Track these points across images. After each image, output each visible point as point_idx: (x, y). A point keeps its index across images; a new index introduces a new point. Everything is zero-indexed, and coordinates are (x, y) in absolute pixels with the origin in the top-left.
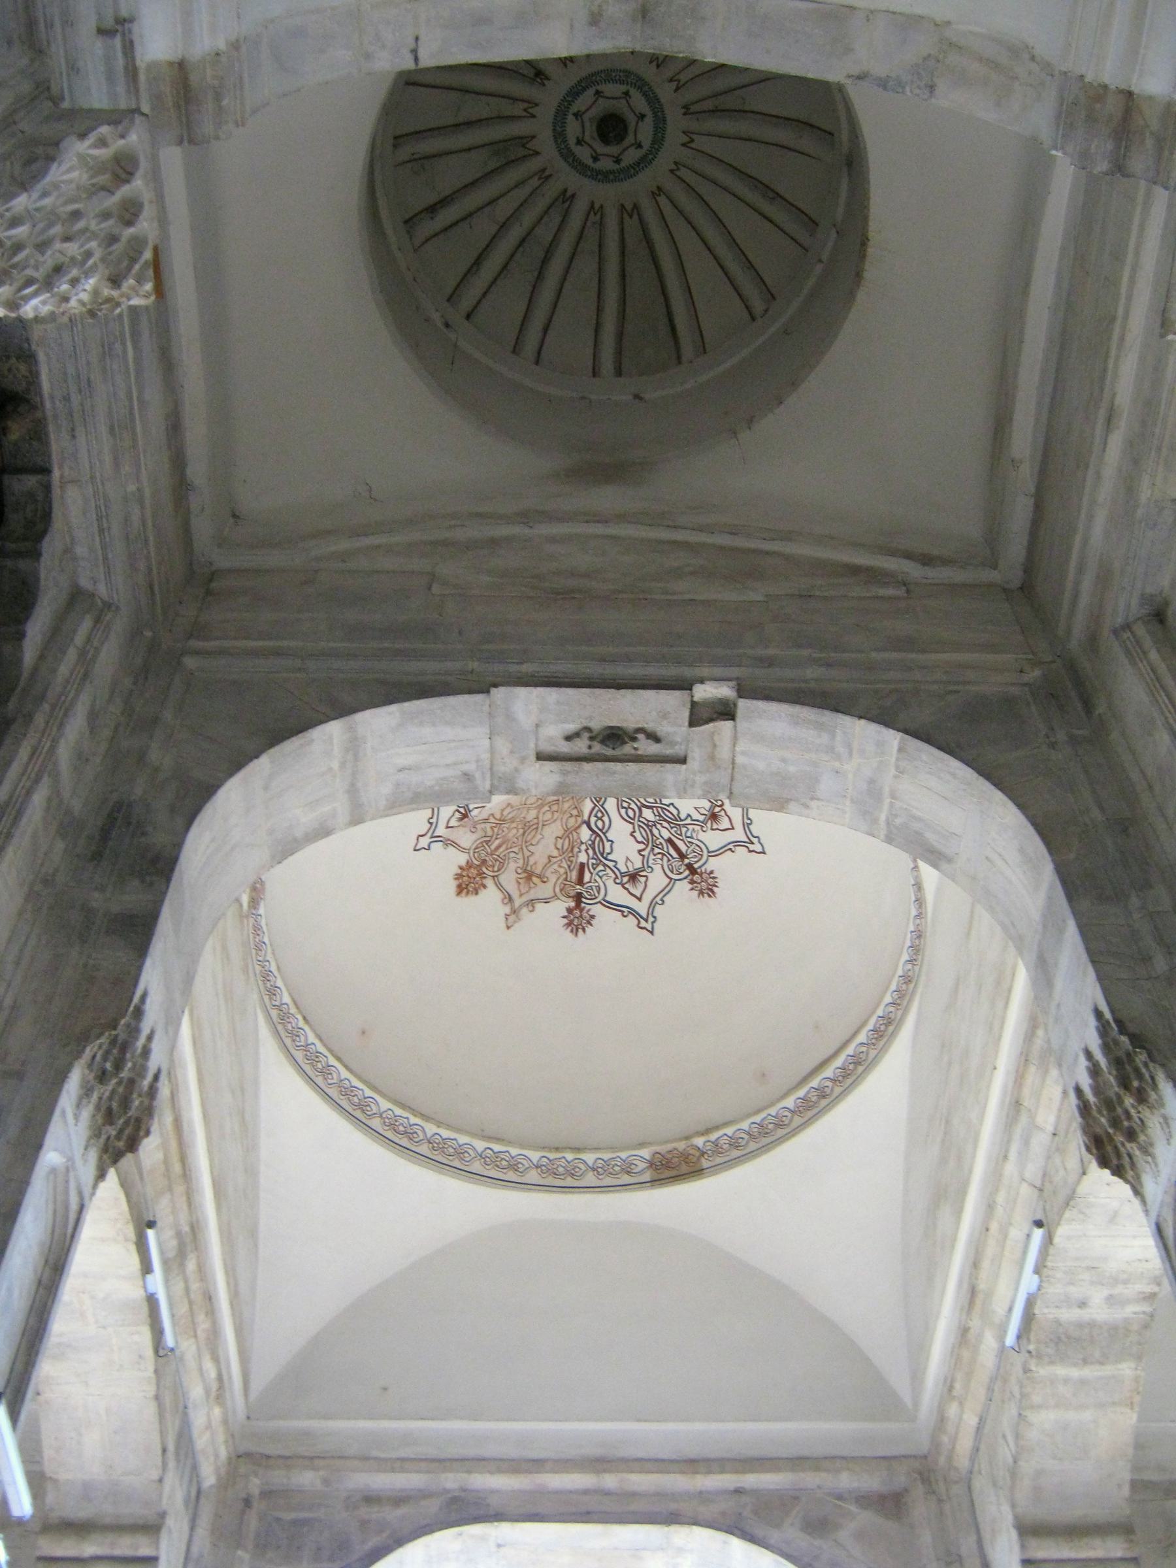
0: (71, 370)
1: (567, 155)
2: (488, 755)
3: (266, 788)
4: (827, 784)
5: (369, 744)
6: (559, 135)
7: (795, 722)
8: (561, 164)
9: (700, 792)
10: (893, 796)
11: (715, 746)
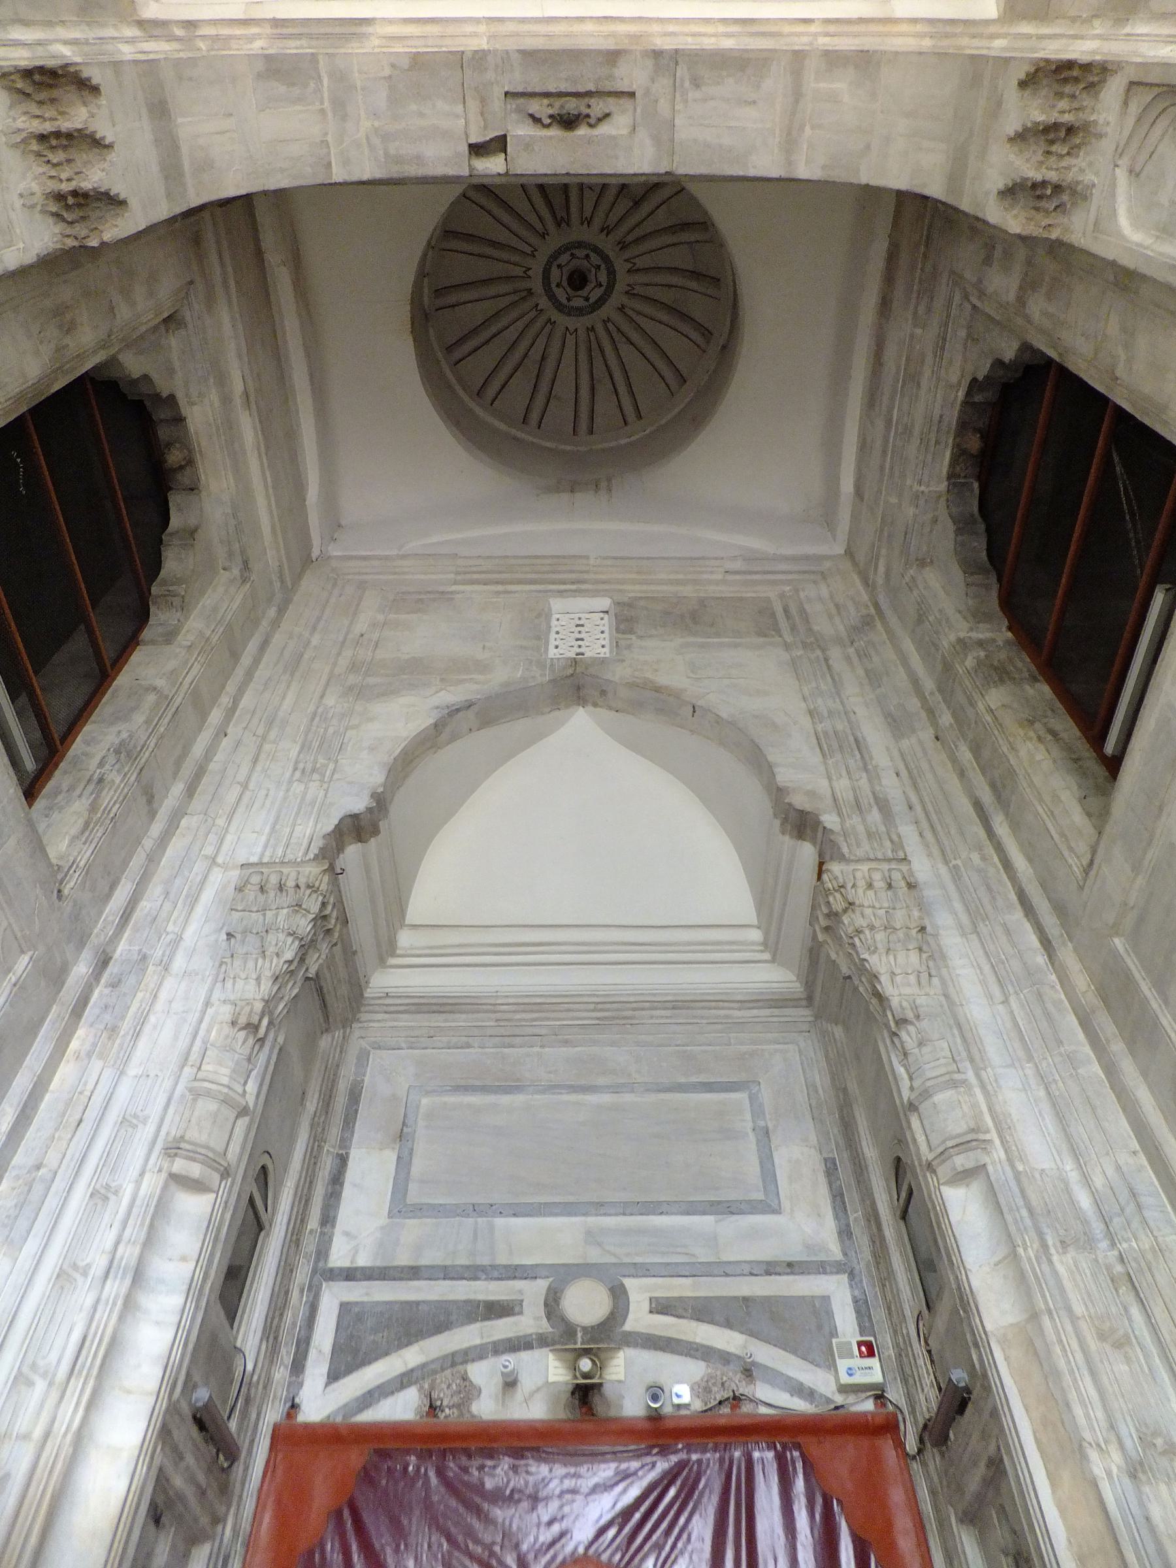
0: (930, 457)
1: (606, 259)
2: (677, 107)
3: (868, 147)
4: (381, 98)
5: (777, 140)
6: (611, 272)
7: (419, 159)
8: (611, 254)
9: (489, 58)
10: (322, 111)
11: (482, 114)
